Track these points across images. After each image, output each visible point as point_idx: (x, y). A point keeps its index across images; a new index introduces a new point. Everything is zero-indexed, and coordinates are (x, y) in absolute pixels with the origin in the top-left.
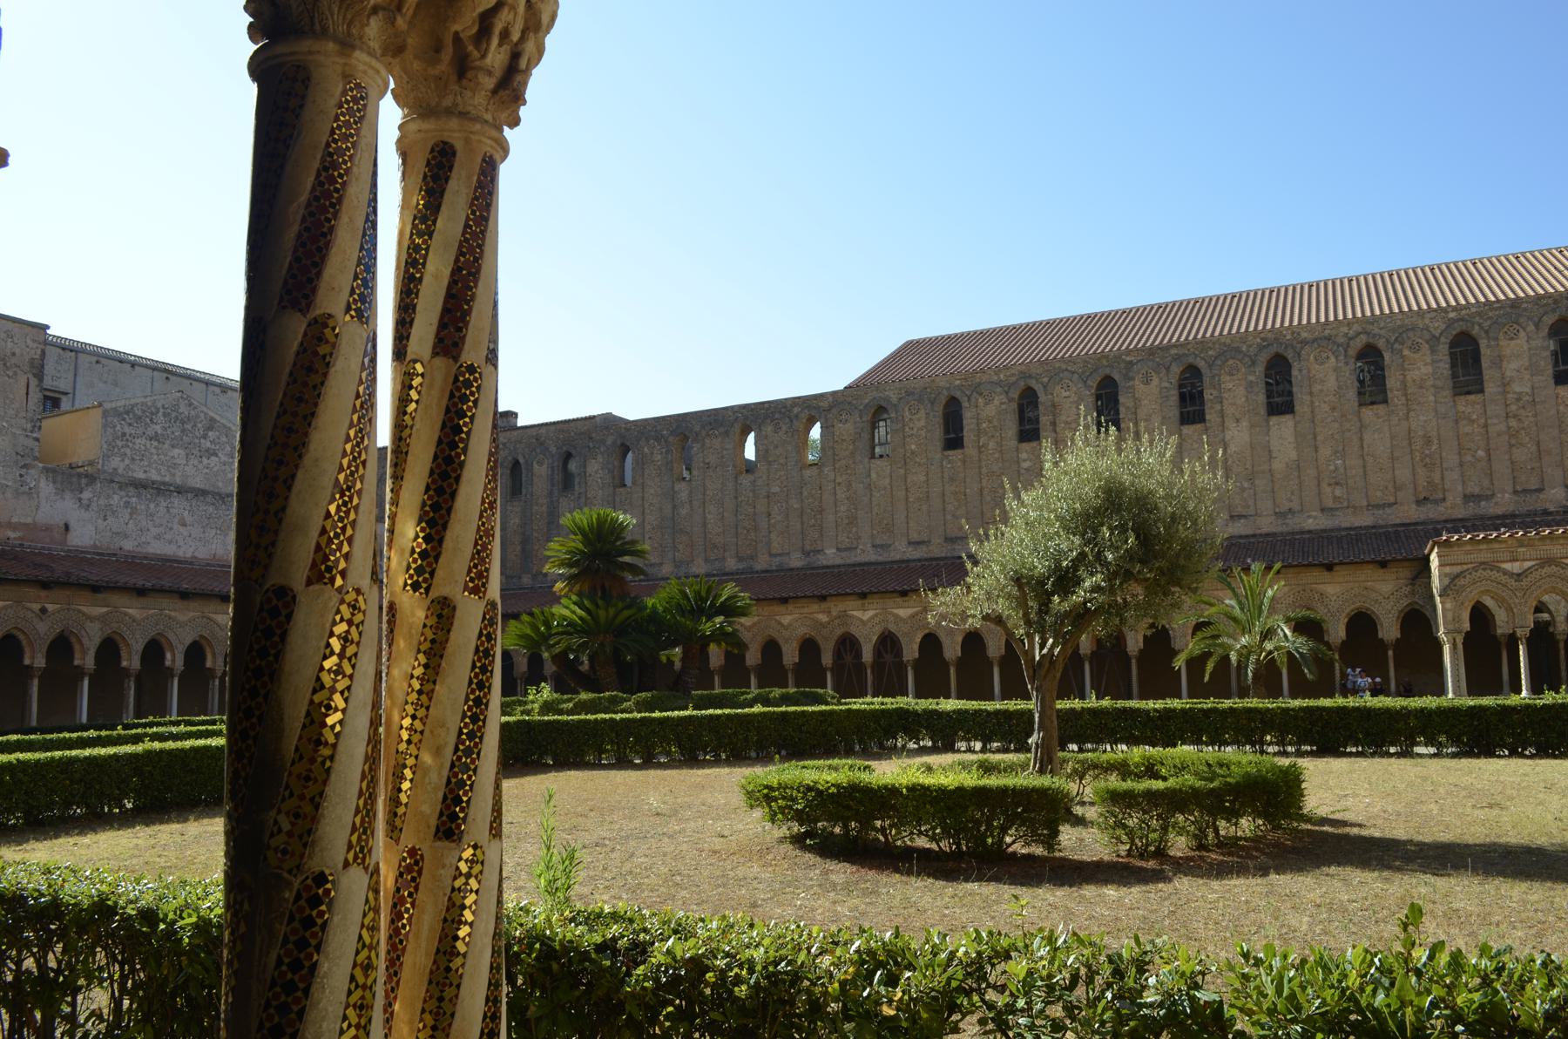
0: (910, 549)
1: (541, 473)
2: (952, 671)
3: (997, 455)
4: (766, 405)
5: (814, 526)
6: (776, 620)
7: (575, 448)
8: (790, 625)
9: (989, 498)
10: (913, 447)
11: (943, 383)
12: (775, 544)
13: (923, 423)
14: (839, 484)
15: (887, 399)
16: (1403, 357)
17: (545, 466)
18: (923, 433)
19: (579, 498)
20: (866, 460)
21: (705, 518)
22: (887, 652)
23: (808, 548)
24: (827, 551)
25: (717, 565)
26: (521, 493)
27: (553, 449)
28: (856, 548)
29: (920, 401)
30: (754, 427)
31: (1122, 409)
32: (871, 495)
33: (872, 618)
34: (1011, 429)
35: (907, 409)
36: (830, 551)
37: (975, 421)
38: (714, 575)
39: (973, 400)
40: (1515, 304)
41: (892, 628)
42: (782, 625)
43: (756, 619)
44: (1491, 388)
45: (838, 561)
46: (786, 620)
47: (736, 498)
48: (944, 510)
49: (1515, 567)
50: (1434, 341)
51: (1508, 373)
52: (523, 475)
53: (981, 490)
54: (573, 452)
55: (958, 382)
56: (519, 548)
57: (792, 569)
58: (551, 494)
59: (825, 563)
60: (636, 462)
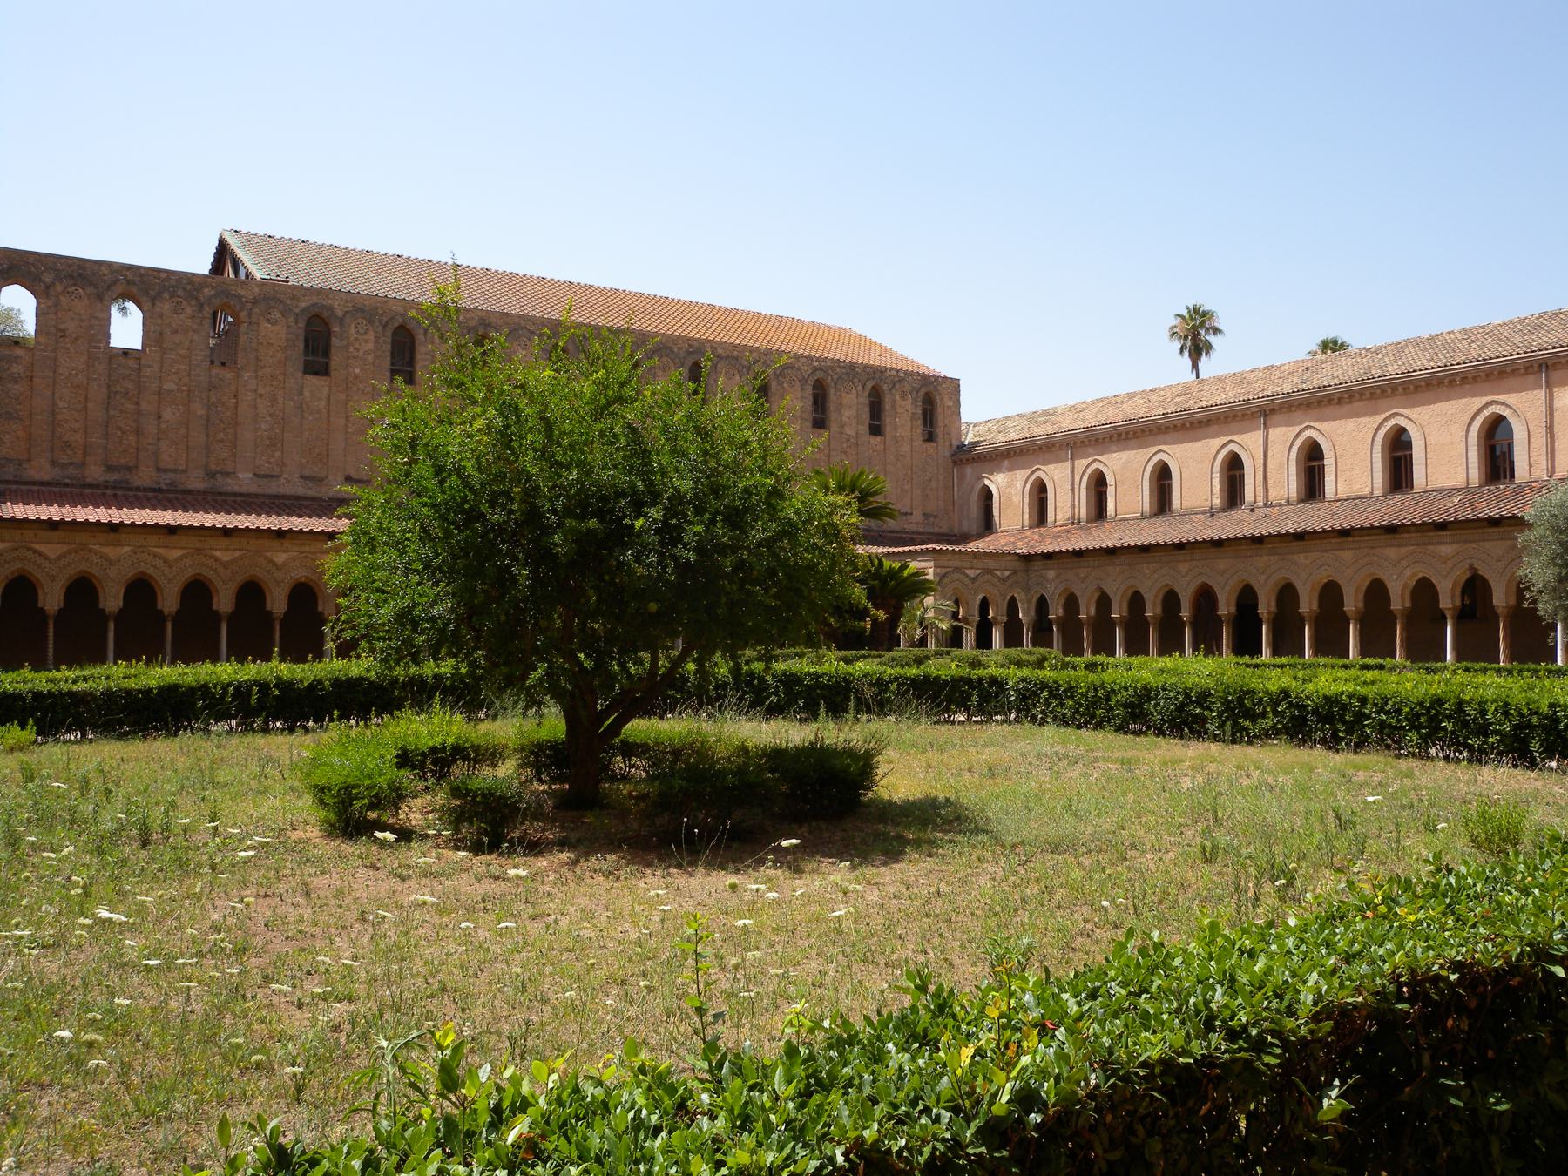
2: (169, 626)
4: (163, 275)
5: (222, 441)
6: (266, 558)
8: (285, 564)
10: (357, 371)
13: (370, 346)
14: (261, 396)
15: (331, 308)
16: (783, 387)
18: (370, 358)
20: (300, 374)
21: (54, 404)
25: (71, 471)
28: (278, 477)
29: (371, 322)
35: (353, 326)
36: (245, 476)
38: (66, 485)
40: (852, 367)
42: (275, 564)
43: (238, 553)
44: (834, 427)
45: (254, 489)
46: (280, 558)
49: (972, 573)
50: (804, 381)
51: (844, 419)
57: (190, 492)
59: (236, 489)
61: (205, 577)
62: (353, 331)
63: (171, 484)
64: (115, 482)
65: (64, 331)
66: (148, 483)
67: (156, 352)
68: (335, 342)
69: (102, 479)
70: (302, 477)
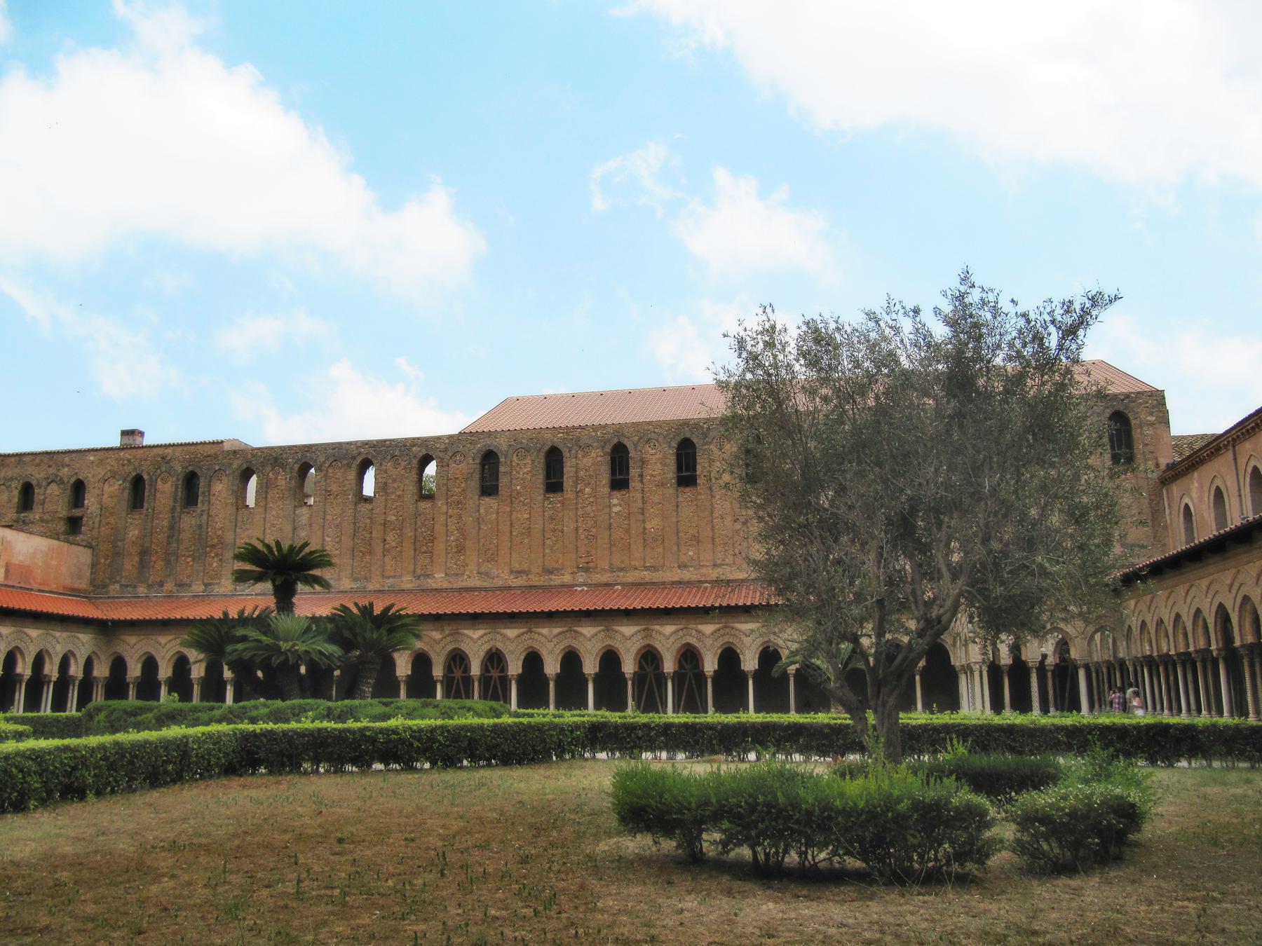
0: (512, 577)
1: (165, 491)
3: (591, 500)
7: (201, 468)
9: (583, 537)
11: (548, 435)
12: (389, 568)
17: (169, 483)
18: (529, 477)
19: (202, 515)
21: (324, 540)
22: (493, 668)
23: (419, 572)
24: (436, 576)
26: (142, 507)
27: (179, 469)
28: (463, 574)
30: (375, 462)
31: (699, 468)
32: (479, 528)
33: (482, 636)
34: (605, 478)
35: (515, 455)
36: (439, 575)
37: (574, 469)
39: (573, 452)
41: (500, 646)
45: (445, 585)
47: (355, 523)
48: (544, 544)
52: (147, 491)
53: (577, 529)
54: (198, 471)
55: (561, 435)
56: (137, 559)
58: (173, 509)
59: (434, 586)
60: (259, 485)
61: (601, 650)
62: (515, 458)
63: (391, 586)
64: (357, 588)
65: (330, 491)
66: (378, 587)
67: (382, 496)
68: (502, 469)
69: (350, 586)
70: (479, 573)
